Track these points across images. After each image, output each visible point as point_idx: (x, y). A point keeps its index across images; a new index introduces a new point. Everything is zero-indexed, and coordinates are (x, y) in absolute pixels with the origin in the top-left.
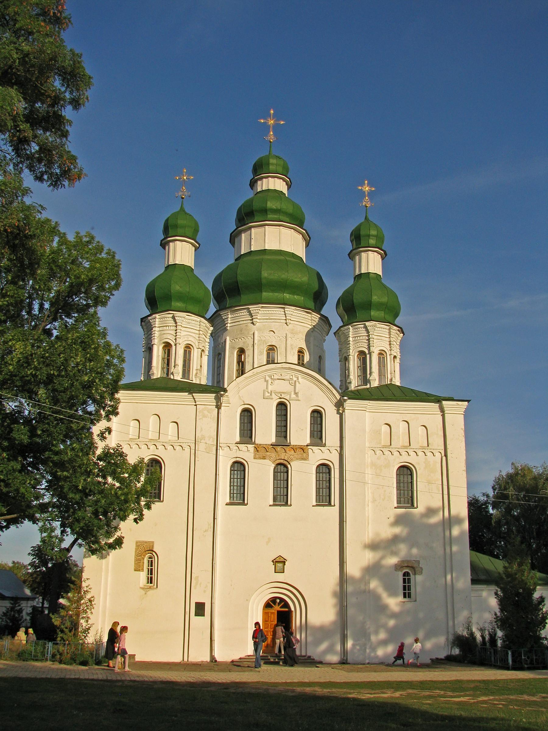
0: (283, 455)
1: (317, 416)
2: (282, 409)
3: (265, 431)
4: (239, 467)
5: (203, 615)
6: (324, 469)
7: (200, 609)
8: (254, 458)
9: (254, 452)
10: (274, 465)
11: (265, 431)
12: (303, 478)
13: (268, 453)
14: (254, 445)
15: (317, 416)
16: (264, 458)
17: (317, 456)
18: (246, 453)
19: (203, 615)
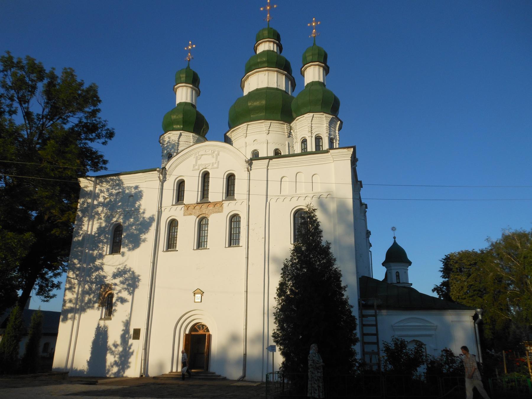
0: (204, 210)
1: (231, 179)
2: (206, 176)
3: (192, 194)
4: (173, 224)
5: (139, 339)
6: (234, 219)
7: (137, 333)
8: (184, 215)
9: (184, 210)
10: (198, 219)
11: (192, 194)
12: (218, 227)
13: (194, 210)
14: (183, 206)
15: (231, 179)
16: (190, 214)
17: (230, 208)
18: (177, 212)
19: (139, 339)
